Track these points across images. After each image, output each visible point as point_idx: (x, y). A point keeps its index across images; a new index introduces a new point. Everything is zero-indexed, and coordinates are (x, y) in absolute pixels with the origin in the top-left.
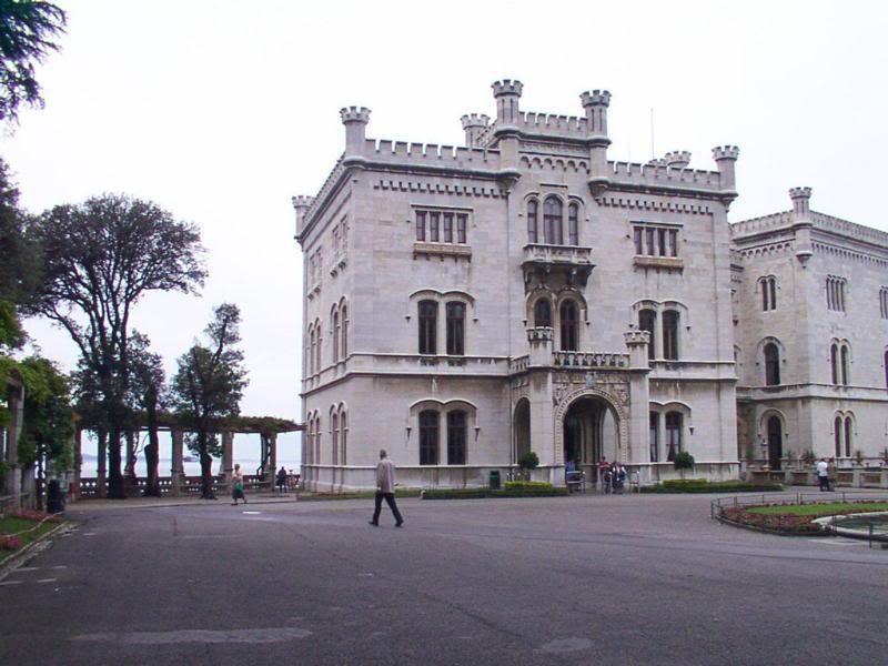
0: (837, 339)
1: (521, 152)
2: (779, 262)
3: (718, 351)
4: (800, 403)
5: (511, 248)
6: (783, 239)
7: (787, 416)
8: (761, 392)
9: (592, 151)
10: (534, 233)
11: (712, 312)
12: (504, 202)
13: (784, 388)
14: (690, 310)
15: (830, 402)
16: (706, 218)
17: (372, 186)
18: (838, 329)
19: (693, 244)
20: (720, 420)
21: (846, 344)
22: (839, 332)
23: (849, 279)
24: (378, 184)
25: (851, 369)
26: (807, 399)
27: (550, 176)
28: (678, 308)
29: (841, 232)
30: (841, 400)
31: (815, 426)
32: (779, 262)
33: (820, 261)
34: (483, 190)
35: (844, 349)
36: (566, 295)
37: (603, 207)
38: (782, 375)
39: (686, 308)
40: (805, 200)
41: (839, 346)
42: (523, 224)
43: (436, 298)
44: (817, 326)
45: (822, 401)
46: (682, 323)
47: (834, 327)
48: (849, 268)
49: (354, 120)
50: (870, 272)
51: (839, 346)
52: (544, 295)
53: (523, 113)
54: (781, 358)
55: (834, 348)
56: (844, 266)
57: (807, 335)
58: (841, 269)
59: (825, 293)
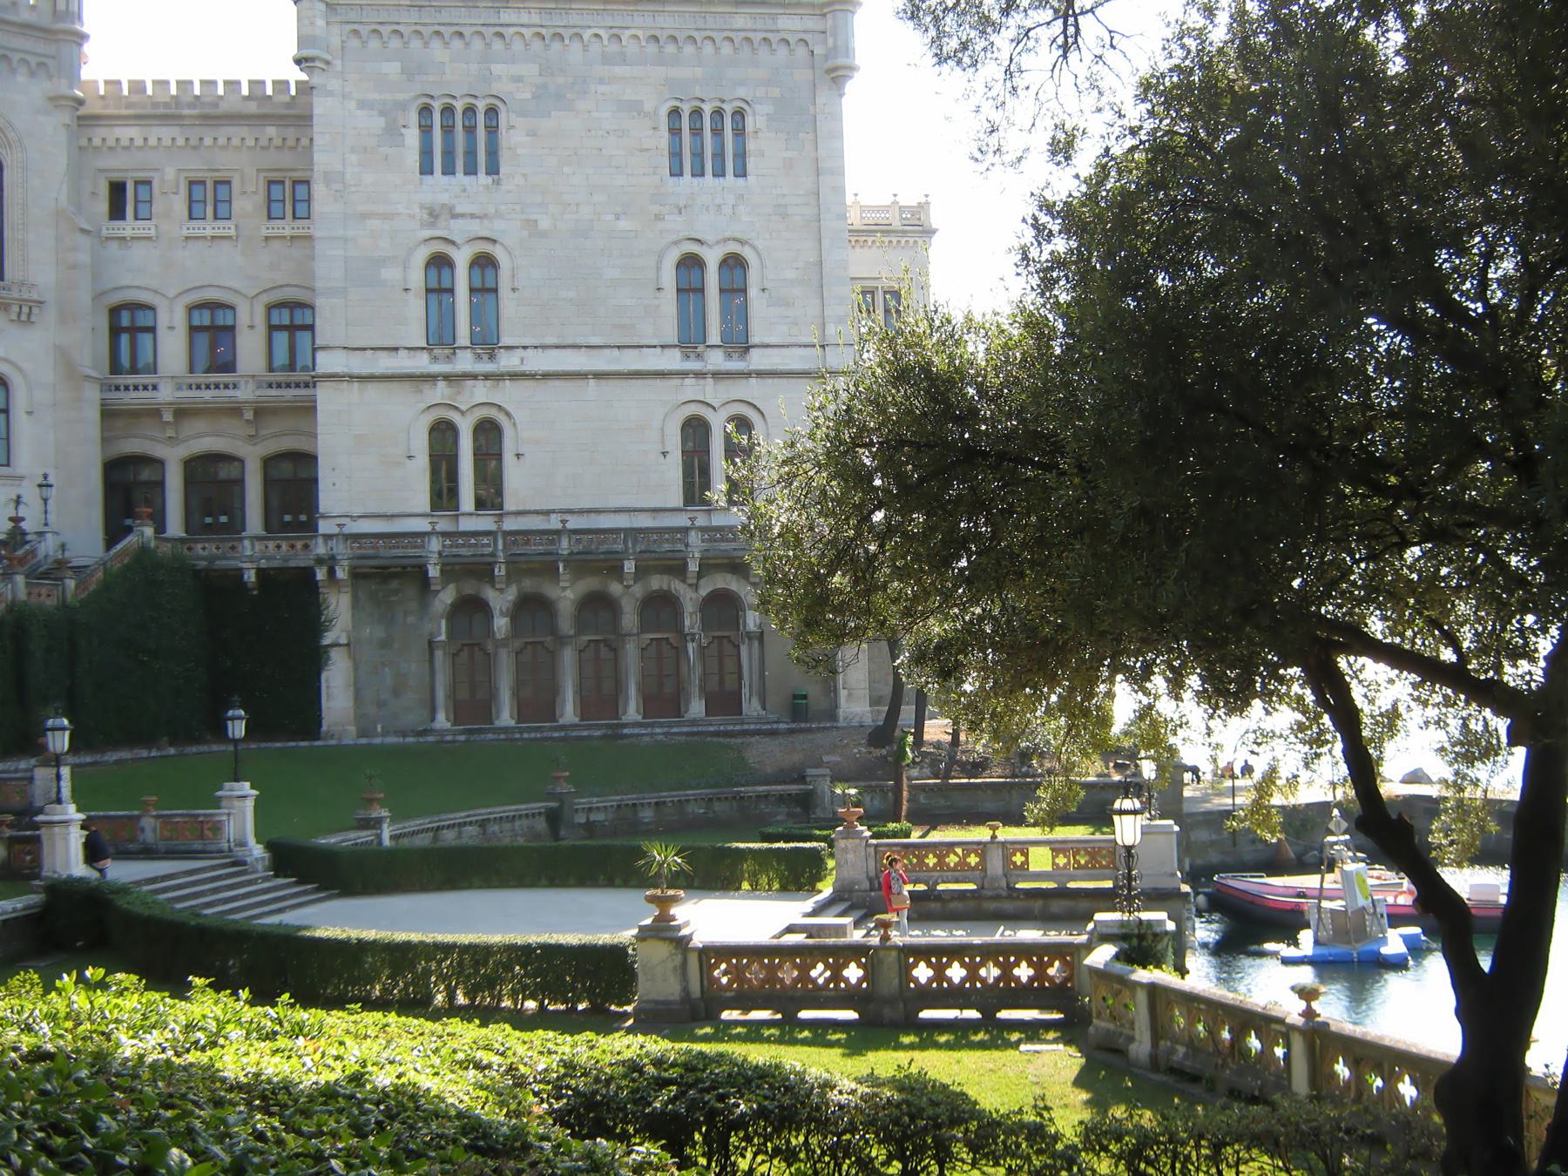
0: (453, 243)
15: (407, 386)
18: (455, 216)
21: (498, 253)
30: (447, 377)
33: (392, 68)
35: (484, 263)
45: (373, 390)
47: (434, 215)
48: (530, 70)
50: (619, 70)
55: (440, 262)
56: (497, 69)
59: (412, 136)
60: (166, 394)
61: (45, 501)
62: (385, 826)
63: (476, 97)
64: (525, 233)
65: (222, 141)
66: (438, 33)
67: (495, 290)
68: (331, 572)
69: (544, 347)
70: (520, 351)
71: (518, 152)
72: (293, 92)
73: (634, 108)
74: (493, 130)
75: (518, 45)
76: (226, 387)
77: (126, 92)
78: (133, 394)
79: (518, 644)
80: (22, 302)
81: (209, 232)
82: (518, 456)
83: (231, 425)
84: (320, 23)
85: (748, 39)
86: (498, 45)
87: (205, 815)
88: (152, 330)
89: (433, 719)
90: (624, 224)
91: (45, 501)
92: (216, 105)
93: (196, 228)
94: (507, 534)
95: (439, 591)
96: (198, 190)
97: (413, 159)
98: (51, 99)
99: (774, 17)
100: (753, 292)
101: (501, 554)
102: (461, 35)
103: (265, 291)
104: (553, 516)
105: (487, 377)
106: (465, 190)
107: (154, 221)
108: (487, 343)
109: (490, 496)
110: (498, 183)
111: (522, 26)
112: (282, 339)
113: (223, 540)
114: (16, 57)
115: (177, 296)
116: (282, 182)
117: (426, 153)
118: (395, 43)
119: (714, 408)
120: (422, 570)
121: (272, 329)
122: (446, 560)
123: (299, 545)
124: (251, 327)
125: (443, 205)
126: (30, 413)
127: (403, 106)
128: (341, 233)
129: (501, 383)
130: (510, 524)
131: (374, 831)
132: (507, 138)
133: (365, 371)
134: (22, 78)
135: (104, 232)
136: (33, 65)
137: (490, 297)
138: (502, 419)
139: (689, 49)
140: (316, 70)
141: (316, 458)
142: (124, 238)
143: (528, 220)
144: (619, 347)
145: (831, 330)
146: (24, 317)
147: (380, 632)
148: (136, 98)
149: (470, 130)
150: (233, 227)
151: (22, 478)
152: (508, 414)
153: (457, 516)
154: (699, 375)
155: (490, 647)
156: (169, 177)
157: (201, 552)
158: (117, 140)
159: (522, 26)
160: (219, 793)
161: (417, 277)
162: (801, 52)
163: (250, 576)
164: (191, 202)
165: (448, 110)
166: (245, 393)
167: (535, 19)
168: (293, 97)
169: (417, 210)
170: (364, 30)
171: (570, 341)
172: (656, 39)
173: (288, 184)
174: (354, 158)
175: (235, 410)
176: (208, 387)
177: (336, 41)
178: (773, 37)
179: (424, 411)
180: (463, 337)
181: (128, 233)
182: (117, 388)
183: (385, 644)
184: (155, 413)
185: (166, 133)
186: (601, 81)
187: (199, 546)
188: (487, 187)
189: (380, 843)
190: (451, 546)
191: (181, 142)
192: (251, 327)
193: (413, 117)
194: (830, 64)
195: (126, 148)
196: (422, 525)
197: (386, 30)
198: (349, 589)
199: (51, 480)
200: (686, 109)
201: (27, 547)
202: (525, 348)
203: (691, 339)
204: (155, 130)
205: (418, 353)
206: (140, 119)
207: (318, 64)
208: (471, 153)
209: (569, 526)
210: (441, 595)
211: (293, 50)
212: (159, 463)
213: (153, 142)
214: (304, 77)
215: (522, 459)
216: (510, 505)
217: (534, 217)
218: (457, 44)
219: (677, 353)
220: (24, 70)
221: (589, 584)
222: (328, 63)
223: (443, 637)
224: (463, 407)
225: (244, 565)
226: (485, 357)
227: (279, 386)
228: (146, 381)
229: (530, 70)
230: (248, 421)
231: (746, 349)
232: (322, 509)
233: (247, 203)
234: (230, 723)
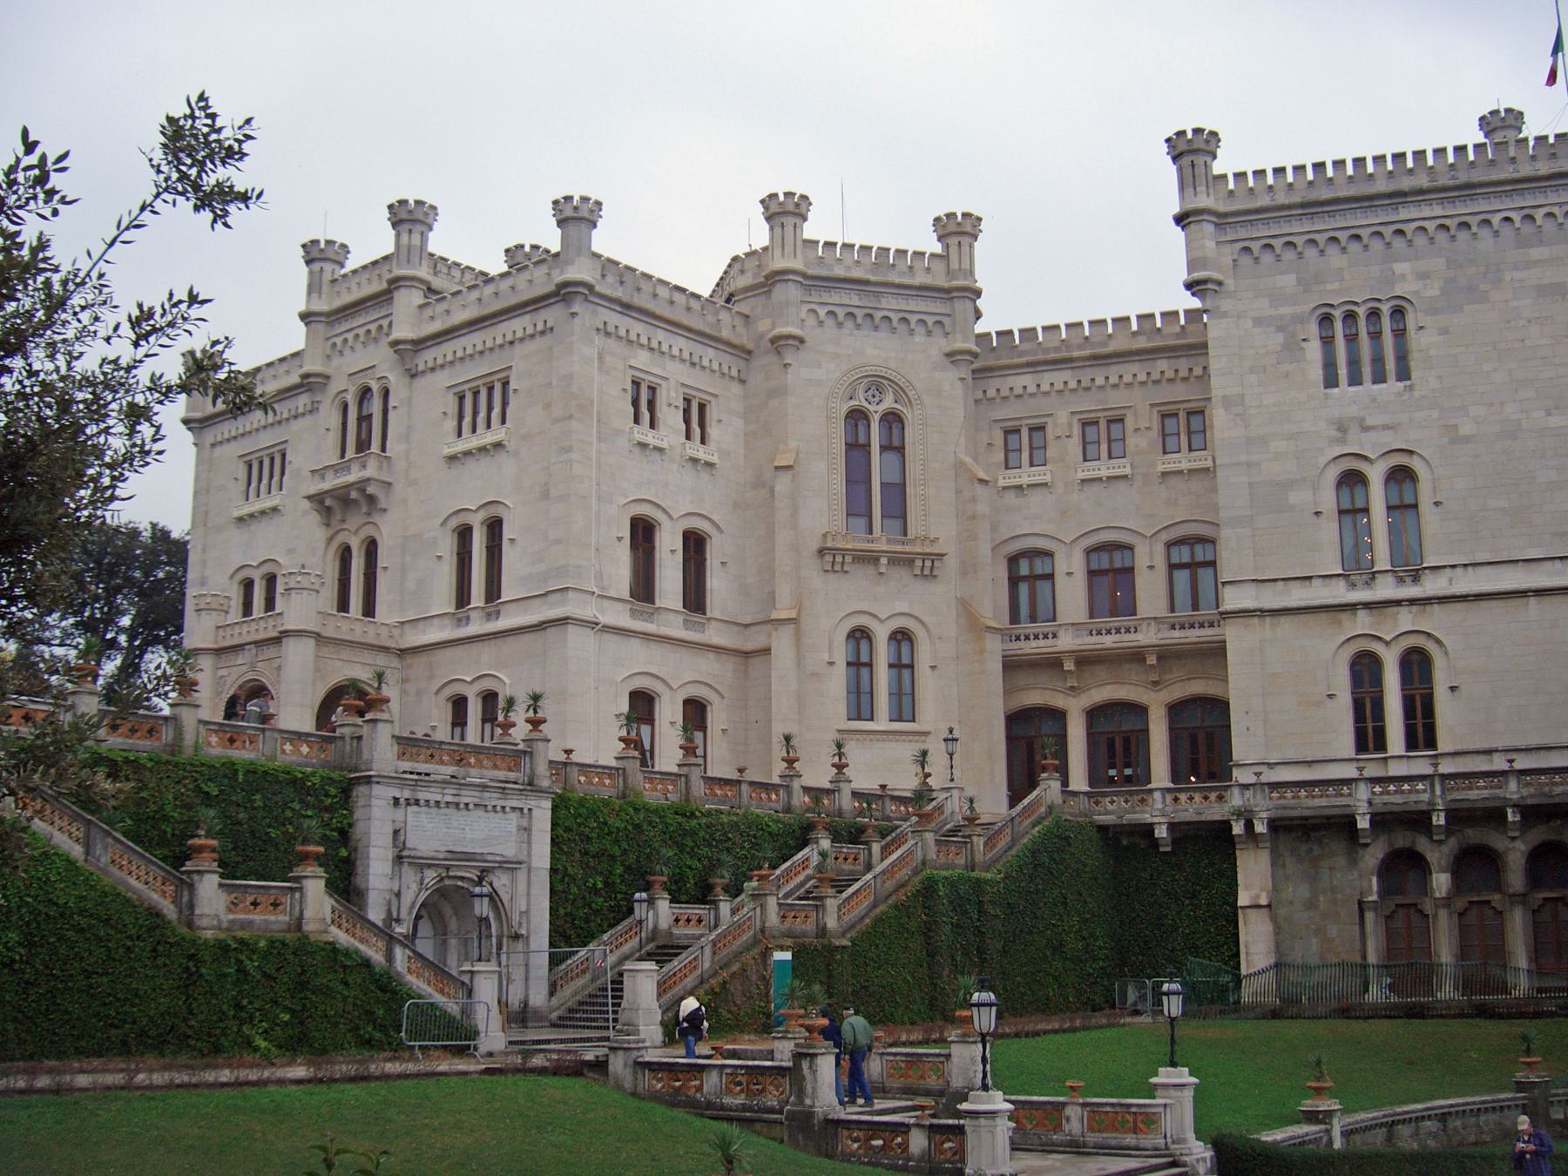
0: (1365, 458)
1: (328, 339)
17: (208, 445)
21: (1416, 464)
22: (1372, 436)
27: (357, 359)
30: (1368, 605)
35: (1401, 476)
36: (368, 531)
40: (1186, 160)
42: (333, 439)
45: (1285, 621)
46: (507, 533)
48: (1437, 264)
50: (1536, 253)
55: (1352, 480)
56: (1401, 268)
59: (1314, 350)
60: (1066, 642)
61: (951, 755)
62: (1335, 1121)
63: (1379, 300)
64: (1446, 440)
65: (1114, 380)
66: (1334, 239)
67: (1415, 506)
68: (1249, 825)
70: (1448, 571)
71: (1432, 352)
72: (1182, 322)
74: (1400, 334)
75: (1420, 241)
76: (1128, 631)
77: (1017, 342)
78: (1034, 643)
79: (1460, 904)
80: (925, 556)
81: (1104, 473)
84: (1210, 244)
86: (1399, 243)
87: (1138, 1106)
88: (1050, 577)
89: (1366, 990)
91: (951, 755)
92: (1105, 344)
94: (1444, 777)
95: (1366, 845)
96: (1091, 430)
97: (1316, 372)
98: (948, 355)
101: (1440, 801)
102: (1357, 237)
103: (1164, 528)
104: (1496, 756)
105: (1412, 602)
106: (1374, 400)
107: (1049, 467)
109: (1421, 733)
110: (1411, 388)
111: (1424, 219)
112: (1182, 577)
113: (1131, 793)
114: (913, 319)
115: (1073, 541)
116: (1176, 415)
117: (1329, 365)
118: (1289, 255)
120: (1350, 821)
121: (1172, 567)
122: (1380, 809)
123: (1213, 796)
124: (1151, 567)
125: (1352, 418)
126: (933, 667)
127: (1300, 320)
128: (1243, 458)
129: (1428, 608)
130: (1446, 767)
131: (1323, 1127)
132: (1416, 341)
133: (1276, 605)
134: (920, 338)
135: (1002, 483)
136: (930, 323)
137: (1410, 514)
138: (1430, 647)
140: (1209, 293)
141: (1227, 704)
142: (1019, 487)
143: (1447, 426)
144: (1561, 558)
146: (927, 572)
147: (1304, 891)
148: (1027, 346)
149: (1376, 336)
150: (1128, 466)
151: (926, 734)
152: (1438, 641)
153: (1386, 758)
155: (1428, 908)
156: (1062, 421)
157: (1110, 807)
158: (1011, 389)
159: (1424, 219)
160: (1154, 1080)
161: (1328, 499)
163: (1161, 832)
164: (1085, 444)
165: (1350, 317)
166: (1146, 637)
168: (1182, 327)
173: (1182, 415)
175: (1136, 656)
176: (1109, 632)
177: (1227, 260)
179: (1343, 643)
181: (1025, 480)
182: (1018, 638)
183: (1311, 905)
184: (1052, 663)
185: (1059, 377)
186: (1516, 267)
187: (1108, 799)
188: (1399, 394)
189: (1330, 1142)
190: (1382, 793)
191: (1073, 384)
192: (1151, 567)
193: (1313, 328)
195: (1019, 396)
196: (1349, 771)
197: (1277, 243)
198: (1268, 844)
199: (956, 734)
201: (934, 803)
202: (1453, 567)
204: (1046, 375)
205: (1334, 580)
206: (1033, 366)
207: (1210, 286)
208: (1378, 361)
209: (1518, 766)
210: (1370, 850)
211: (1183, 275)
212: (1059, 716)
213: (1045, 387)
214: (1196, 303)
215: (1456, 693)
216: (1444, 745)
217: (1452, 422)
218: (1355, 247)
220: (920, 330)
221: (1538, 835)
222: (1220, 283)
223: (1374, 897)
224: (1388, 638)
225: (1156, 820)
226: (1408, 580)
227: (1182, 627)
228: (1046, 630)
230: (1152, 666)
232: (1235, 757)
233: (1141, 437)
234: (1165, 999)
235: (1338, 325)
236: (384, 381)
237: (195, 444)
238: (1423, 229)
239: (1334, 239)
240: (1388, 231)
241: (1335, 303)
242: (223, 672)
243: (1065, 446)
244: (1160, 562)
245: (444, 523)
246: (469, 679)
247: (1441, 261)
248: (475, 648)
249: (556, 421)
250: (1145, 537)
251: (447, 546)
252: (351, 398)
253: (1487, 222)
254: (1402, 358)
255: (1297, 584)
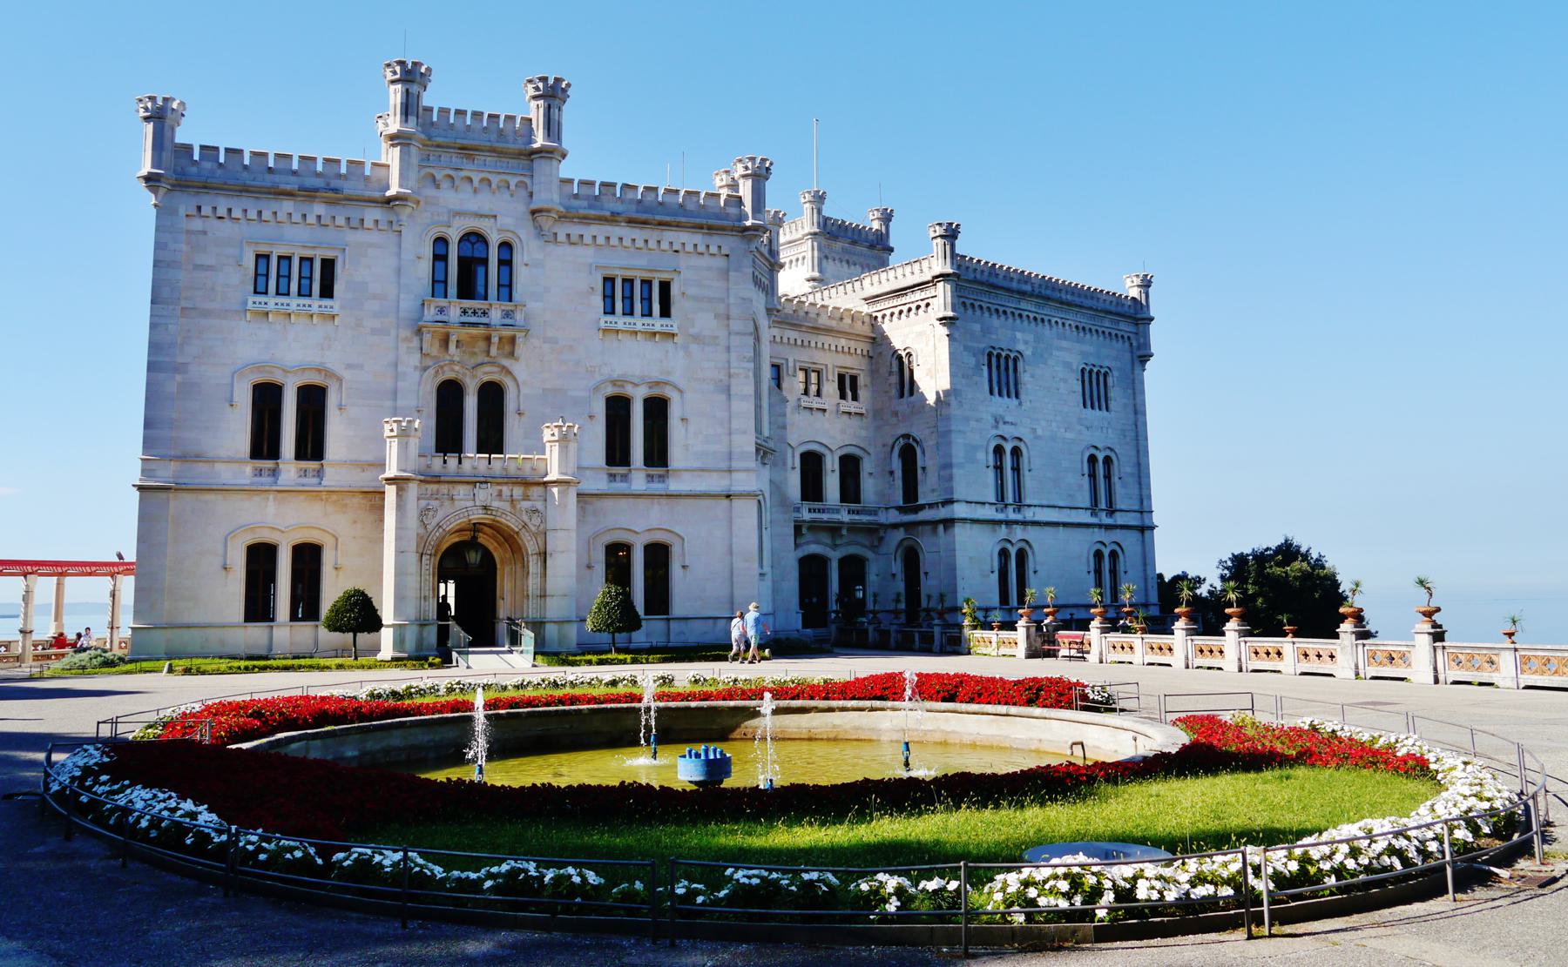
0: (1004, 438)
2: (918, 328)
3: (730, 453)
4: (941, 527)
5: (401, 303)
6: (923, 295)
7: (928, 545)
8: (897, 513)
9: (536, 164)
10: (438, 284)
11: (723, 397)
12: (392, 237)
13: (922, 507)
14: (688, 395)
15: (990, 526)
16: (720, 262)
18: (1005, 423)
19: (696, 298)
20: (731, 554)
23: (1028, 352)
24: (194, 212)
25: (1028, 480)
26: (949, 523)
28: (668, 392)
29: (1014, 285)
30: (1008, 523)
31: (961, 561)
32: (918, 328)
33: (977, 327)
34: (362, 221)
35: (1016, 452)
37: (551, 247)
38: (920, 489)
39: (681, 391)
41: (1008, 447)
42: (424, 268)
43: (277, 378)
44: (967, 419)
45: (976, 526)
46: (675, 412)
47: (997, 421)
48: (1030, 337)
49: (161, 116)
50: (1064, 344)
51: (1008, 447)
52: (449, 375)
53: (430, 110)
54: (920, 464)
55: (999, 450)
56: (1019, 335)
57: (950, 431)
58: (1014, 339)
59: (985, 368)
65: (820, 345)
69: (1042, 506)
73: (1067, 365)
75: (1026, 322)
81: (815, 406)
82: (1035, 572)
83: (825, 537)
85: (1110, 334)
86: (1018, 321)
90: (1069, 435)
93: (805, 402)
99: (1118, 321)
100: (1115, 479)
102: (1005, 312)
108: (1019, 505)
110: (1020, 404)
118: (978, 312)
119: (1105, 546)
138: (1027, 548)
139: (1088, 336)
144: (1070, 508)
145: (1145, 503)
149: (1007, 368)
152: (1030, 546)
154: (1100, 526)
162: (1127, 344)
165: (999, 356)
167: (1033, 309)
169: (990, 418)
170: (968, 302)
171: (1052, 503)
172: (1077, 327)
174: (964, 381)
175: (834, 529)
178: (1120, 334)
180: (1010, 499)
185: (792, 335)
191: (799, 342)
194: (1142, 353)
200: (1088, 369)
203: (1094, 508)
213: (785, 340)
218: (1003, 317)
219: (1089, 512)
224: (1014, 541)
229: (1030, 337)
231: (1111, 512)
233: (830, 388)
235: (994, 360)
236: (510, 235)
237: (156, 206)
238: (1028, 316)
239: (997, 310)
240: (1017, 312)
241: (997, 346)
242: (423, 503)
243: (793, 384)
244: (837, 467)
245: (596, 389)
246: (636, 530)
247: (1032, 336)
248: (641, 502)
249: (737, 333)
250: (830, 449)
251: (600, 409)
252: (454, 236)
253: (1050, 321)
254: (1016, 384)
255: (978, 506)
